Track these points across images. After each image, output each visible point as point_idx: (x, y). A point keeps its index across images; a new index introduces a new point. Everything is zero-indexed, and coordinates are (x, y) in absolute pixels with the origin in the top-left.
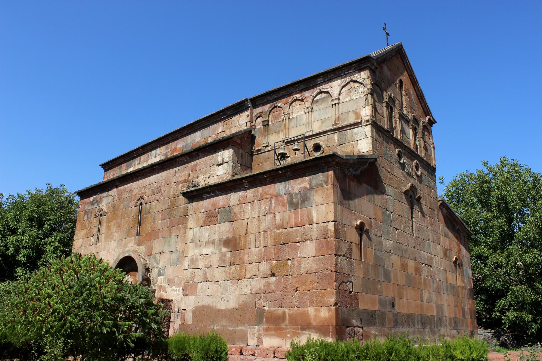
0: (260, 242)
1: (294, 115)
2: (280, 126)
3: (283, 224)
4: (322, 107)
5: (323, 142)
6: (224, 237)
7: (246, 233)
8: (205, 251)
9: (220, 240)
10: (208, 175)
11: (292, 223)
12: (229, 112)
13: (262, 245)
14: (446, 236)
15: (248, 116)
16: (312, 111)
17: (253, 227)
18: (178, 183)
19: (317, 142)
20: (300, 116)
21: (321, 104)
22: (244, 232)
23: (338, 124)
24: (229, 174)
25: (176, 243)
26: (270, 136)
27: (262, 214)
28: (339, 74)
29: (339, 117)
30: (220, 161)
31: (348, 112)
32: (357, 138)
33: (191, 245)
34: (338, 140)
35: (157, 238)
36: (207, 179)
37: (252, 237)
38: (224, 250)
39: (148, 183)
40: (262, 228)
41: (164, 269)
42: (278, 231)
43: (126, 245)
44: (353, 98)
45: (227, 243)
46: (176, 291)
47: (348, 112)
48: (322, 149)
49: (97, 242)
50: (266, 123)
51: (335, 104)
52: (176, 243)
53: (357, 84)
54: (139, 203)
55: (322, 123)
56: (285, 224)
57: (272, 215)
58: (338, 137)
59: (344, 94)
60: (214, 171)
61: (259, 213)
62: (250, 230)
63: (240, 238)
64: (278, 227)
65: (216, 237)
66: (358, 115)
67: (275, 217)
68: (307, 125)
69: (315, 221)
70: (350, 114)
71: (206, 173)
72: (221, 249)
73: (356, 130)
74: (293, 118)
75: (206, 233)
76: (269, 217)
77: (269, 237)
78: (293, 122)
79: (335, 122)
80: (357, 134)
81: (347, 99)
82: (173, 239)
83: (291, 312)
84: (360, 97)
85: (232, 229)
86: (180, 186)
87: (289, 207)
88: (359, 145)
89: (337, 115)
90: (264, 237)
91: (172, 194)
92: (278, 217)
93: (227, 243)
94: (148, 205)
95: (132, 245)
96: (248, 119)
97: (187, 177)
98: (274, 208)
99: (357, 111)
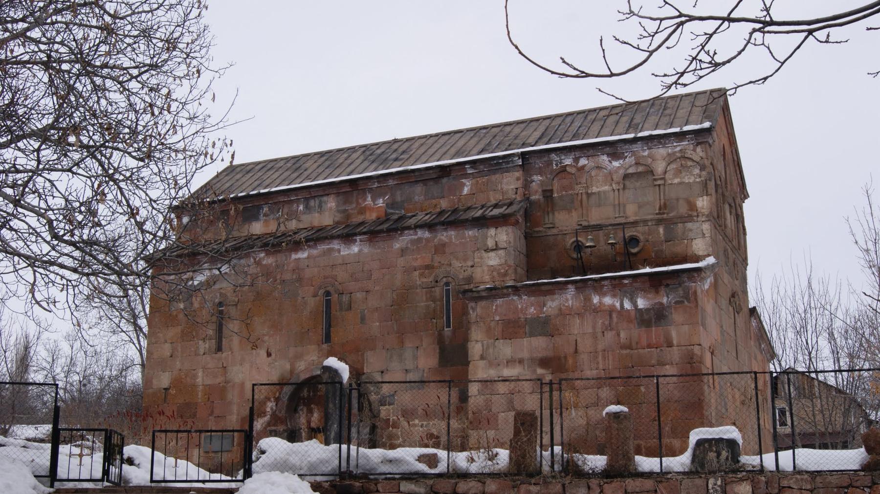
0: (598, 363)
1: (595, 189)
2: (573, 202)
3: (631, 343)
4: (638, 184)
5: (643, 234)
6: (540, 355)
7: (576, 351)
8: (507, 372)
9: (532, 360)
10: (470, 263)
11: (644, 342)
12: (482, 167)
13: (601, 366)
14: (756, 359)
15: (518, 179)
16: (624, 188)
17: (585, 345)
18: (409, 270)
19: (635, 234)
20: (604, 192)
21: (637, 181)
22: (572, 350)
23: (664, 213)
24: (510, 266)
25: (415, 358)
26: (556, 214)
27: (599, 330)
28: (665, 143)
29: (665, 204)
30: (490, 243)
31: (677, 200)
32: (691, 235)
33: (482, 363)
34: (664, 234)
35: (373, 349)
36: (469, 269)
37: (584, 358)
38: (540, 371)
39: (340, 261)
40: (600, 347)
41: (393, 395)
42: (625, 352)
43: (298, 357)
44: (684, 180)
45: (544, 362)
46: (422, 426)
47: (677, 200)
48: (641, 244)
49: (219, 349)
50: (548, 194)
51: (659, 185)
52: (415, 358)
53: (690, 163)
54: (321, 292)
55: (640, 207)
56: (634, 344)
57: (614, 332)
58: (664, 230)
59: (672, 172)
60: (481, 258)
61: (594, 327)
62: (580, 348)
63: (565, 357)
64: (624, 347)
65: (525, 354)
66: (692, 206)
67: (619, 335)
68: (617, 208)
69: (675, 342)
70: (681, 202)
71: (465, 260)
72: (535, 371)
73: (689, 225)
74: (594, 193)
75: (506, 349)
76: (610, 335)
77: (611, 357)
78: (593, 199)
79: (660, 209)
80: (691, 230)
81: (676, 181)
82: (408, 354)
83: (649, 445)
84: (695, 182)
85: (552, 345)
86: (417, 273)
87: (638, 324)
88: (694, 246)
89: (662, 201)
90: (604, 358)
91: (398, 283)
92: (622, 335)
93: (544, 362)
94: (345, 298)
95: (315, 358)
96: (519, 184)
97: (427, 262)
98: (617, 323)
99: (691, 199)
